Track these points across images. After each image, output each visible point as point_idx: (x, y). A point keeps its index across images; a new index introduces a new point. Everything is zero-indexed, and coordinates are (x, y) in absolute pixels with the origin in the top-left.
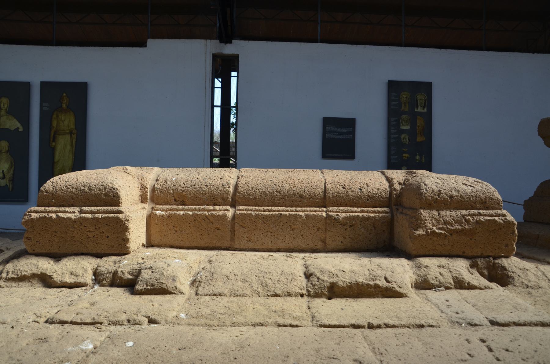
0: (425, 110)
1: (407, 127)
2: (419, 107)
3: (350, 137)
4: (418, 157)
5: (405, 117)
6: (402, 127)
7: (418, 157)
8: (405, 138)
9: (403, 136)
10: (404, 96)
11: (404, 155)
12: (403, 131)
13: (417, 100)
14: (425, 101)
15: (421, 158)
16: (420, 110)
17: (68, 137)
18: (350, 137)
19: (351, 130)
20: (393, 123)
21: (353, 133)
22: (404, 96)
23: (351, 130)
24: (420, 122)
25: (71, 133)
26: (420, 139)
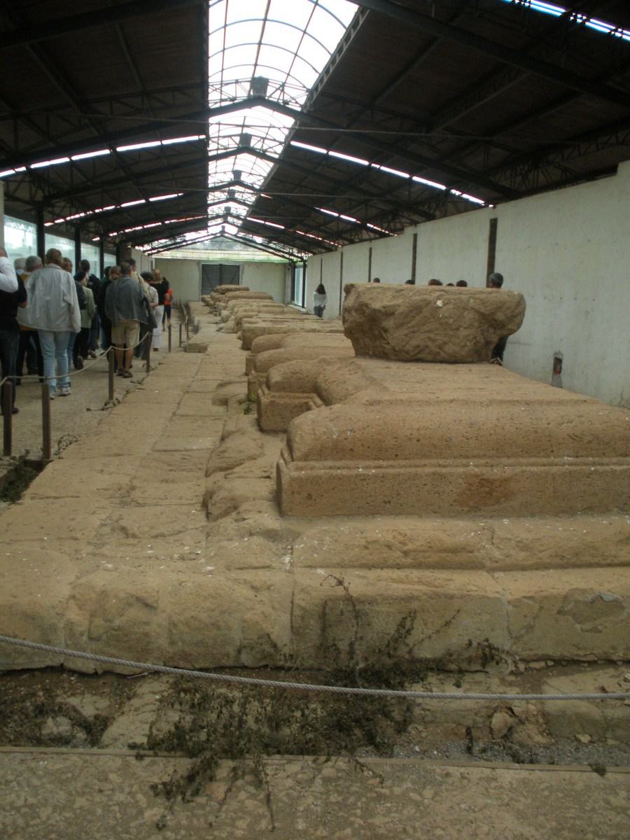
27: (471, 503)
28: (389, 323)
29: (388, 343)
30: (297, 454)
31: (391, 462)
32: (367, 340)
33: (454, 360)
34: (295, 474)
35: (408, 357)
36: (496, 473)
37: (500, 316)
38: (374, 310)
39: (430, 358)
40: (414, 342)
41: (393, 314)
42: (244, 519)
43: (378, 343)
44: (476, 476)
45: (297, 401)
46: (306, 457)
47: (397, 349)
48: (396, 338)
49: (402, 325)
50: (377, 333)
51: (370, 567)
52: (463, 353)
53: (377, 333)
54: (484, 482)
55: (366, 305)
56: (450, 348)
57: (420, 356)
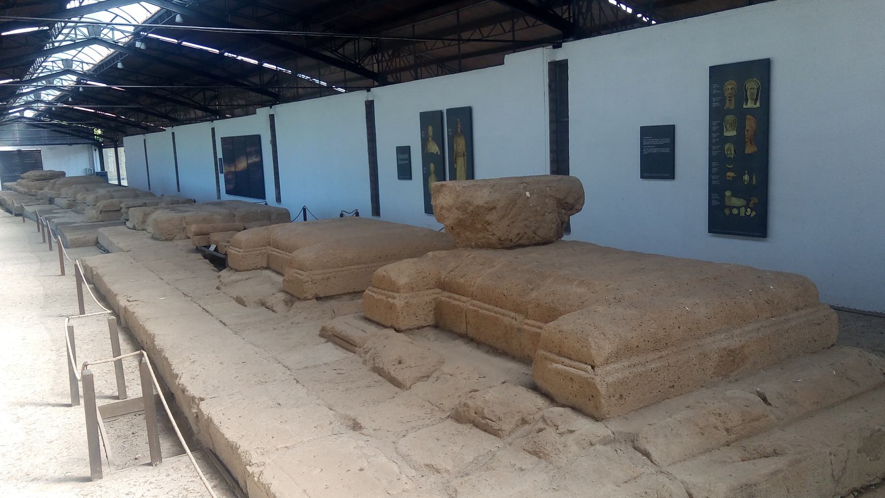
0: (758, 104)
1: (731, 133)
2: (749, 101)
3: (667, 150)
4: (746, 177)
5: (729, 118)
6: (726, 134)
7: (746, 177)
8: (729, 149)
9: (727, 146)
10: (730, 86)
11: (728, 174)
12: (728, 139)
13: (746, 91)
14: (758, 90)
15: (751, 179)
16: (750, 105)
17: (462, 158)
18: (667, 150)
19: (668, 141)
20: (714, 128)
21: (672, 145)
22: (730, 86)
23: (668, 141)
24: (750, 124)
25: (464, 155)
26: (750, 149)
27: (723, 373)
28: (491, 217)
29: (494, 234)
30: (598, 360)
31: (667, 352)
32: (468, 234)
33: (545, 242)
34: (610, 379)
35: (512, 244)
36: (735, 343)
37: (570, 200)
38: (478, 206)
39: (527, 242)
40: (515, 231)
41: (494, 208)
42: (572, 432)
43: (480, 235)
44: (725, 349)
45: (427, 299)
46: (607, 362)
47: (503, 239)
48: (500, 229)
49: (503, 217)
50: (479, 226)
51: (709, 450)
52: (552, 235)
53: (479, 226)
54: (731, 352)
55: (469, 203)
56: (542, 233)
57: (521, 242)
